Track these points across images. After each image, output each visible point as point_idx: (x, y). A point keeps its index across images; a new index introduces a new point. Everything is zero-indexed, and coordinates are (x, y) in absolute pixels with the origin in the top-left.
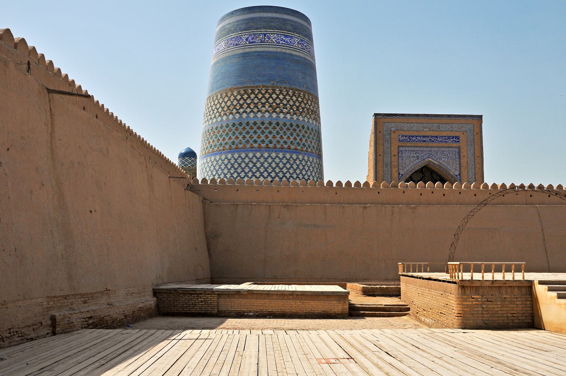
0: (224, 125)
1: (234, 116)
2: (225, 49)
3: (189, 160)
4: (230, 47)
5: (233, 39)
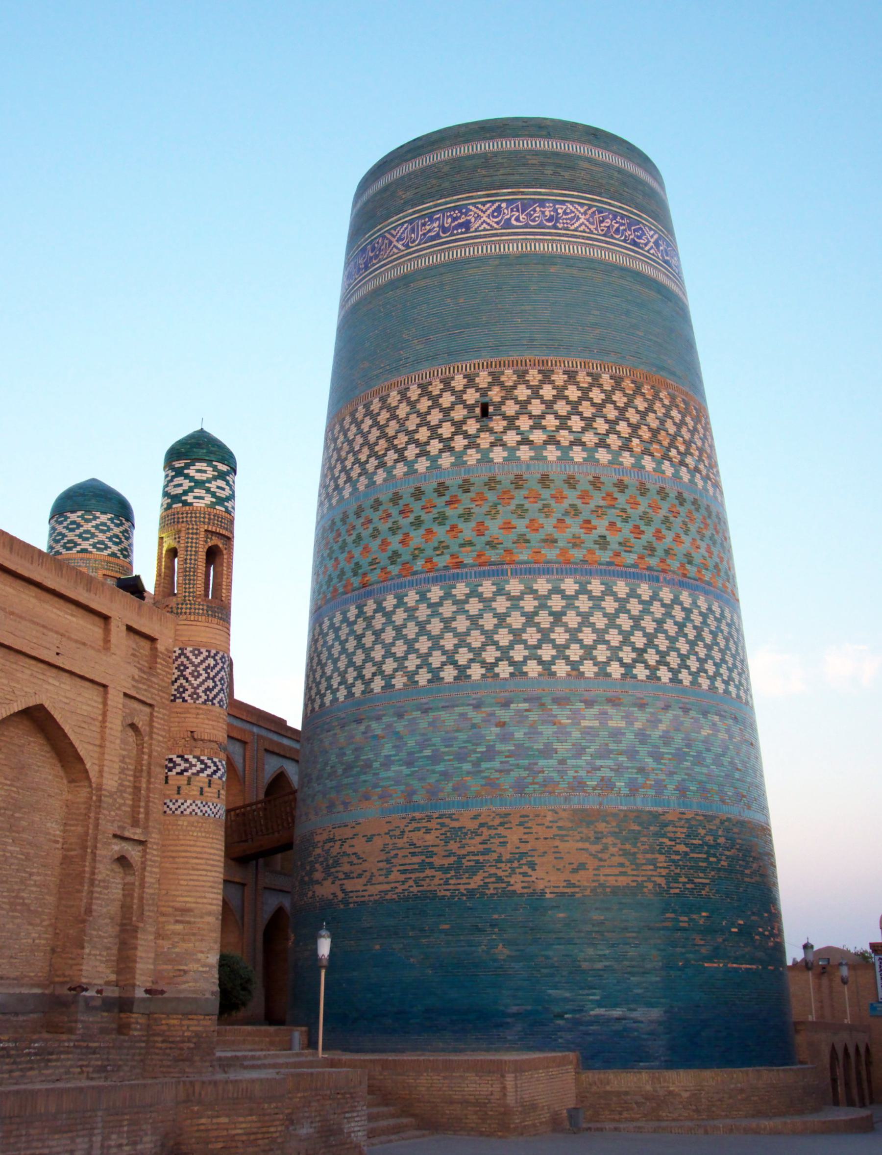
2: (591, 232)
3: (112, 526)
5: (618, 219)
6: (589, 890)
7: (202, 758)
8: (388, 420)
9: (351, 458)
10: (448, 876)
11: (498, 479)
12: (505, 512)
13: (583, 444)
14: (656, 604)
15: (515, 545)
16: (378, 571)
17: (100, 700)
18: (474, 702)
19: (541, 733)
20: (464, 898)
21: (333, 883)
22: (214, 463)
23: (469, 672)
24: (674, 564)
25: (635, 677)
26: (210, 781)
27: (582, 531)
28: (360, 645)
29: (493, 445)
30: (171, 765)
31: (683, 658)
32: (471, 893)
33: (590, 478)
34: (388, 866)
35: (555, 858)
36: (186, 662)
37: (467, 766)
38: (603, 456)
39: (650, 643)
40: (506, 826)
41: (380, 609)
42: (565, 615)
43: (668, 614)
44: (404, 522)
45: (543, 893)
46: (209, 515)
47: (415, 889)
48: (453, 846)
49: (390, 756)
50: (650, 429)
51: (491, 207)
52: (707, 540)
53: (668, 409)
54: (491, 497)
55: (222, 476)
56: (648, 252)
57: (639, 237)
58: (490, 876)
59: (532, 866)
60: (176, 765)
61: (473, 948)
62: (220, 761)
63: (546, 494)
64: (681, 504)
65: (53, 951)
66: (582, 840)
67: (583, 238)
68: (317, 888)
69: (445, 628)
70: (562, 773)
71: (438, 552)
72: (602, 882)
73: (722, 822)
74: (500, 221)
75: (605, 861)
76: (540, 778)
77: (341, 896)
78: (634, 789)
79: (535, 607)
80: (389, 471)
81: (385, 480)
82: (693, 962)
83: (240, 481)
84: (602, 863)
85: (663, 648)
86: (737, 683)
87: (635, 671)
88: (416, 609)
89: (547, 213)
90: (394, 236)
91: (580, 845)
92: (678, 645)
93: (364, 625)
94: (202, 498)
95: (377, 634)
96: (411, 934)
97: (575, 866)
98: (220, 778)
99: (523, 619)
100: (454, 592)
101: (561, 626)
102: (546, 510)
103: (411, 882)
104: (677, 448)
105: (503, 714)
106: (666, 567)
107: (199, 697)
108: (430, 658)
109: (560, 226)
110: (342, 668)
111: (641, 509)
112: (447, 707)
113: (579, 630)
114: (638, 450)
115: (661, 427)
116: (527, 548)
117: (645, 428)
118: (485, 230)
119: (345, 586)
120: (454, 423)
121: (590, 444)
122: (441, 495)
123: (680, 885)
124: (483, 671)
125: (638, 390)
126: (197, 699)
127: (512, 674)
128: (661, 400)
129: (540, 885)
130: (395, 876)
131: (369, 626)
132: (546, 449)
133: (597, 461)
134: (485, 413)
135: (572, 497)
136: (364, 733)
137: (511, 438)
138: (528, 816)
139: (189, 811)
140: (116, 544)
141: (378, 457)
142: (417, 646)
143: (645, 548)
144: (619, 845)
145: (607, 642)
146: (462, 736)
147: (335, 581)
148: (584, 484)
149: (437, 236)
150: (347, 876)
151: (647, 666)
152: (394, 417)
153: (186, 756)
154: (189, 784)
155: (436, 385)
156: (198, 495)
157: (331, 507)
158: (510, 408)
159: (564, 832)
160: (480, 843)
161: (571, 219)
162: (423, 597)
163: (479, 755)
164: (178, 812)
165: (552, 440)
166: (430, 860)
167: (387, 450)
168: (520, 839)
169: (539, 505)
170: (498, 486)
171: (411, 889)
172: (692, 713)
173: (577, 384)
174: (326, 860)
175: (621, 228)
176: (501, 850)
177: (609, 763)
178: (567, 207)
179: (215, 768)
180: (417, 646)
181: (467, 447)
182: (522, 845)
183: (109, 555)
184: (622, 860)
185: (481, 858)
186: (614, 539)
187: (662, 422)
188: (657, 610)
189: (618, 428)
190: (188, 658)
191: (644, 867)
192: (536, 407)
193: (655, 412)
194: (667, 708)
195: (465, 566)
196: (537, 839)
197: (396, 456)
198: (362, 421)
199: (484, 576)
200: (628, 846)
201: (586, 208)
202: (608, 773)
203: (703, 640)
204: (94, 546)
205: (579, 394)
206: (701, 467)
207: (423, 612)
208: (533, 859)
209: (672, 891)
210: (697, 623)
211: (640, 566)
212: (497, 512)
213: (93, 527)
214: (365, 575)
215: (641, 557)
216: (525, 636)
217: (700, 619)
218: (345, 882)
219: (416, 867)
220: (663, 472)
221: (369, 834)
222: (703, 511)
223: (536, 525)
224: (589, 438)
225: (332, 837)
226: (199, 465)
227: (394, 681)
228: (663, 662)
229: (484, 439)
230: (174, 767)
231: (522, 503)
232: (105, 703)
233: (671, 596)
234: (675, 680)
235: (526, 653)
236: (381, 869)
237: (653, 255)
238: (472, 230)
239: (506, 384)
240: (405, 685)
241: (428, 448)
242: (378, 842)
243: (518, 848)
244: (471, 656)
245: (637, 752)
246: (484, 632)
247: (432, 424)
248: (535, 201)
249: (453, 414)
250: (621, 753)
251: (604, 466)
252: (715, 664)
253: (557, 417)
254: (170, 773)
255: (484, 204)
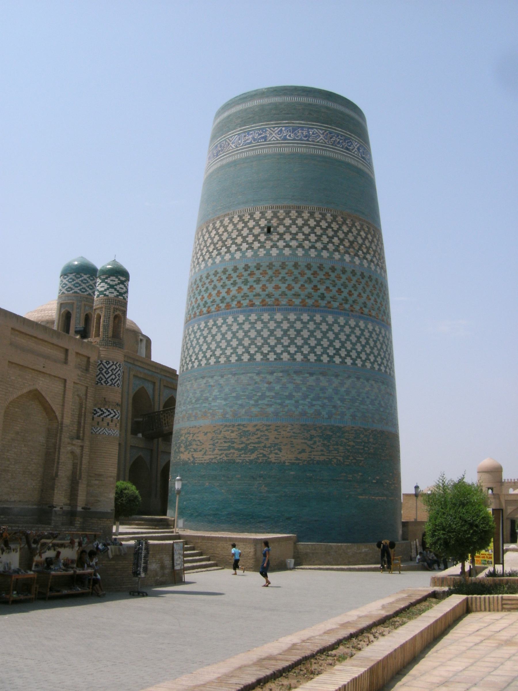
0: (349, 270)
1: (361, 262)
2: (326, 143)
3: (89, 281)
4: (336, 146)
6: (306, 462)
7: (109, 409)
8: (223, 232)
9: (205, 250)
10: (241, 453)
11: (274, 264)
12: (276, 281)
13: (315, 248)
14: (347, 327)
15: (280, 297)
16: (215, 306)
17: (63, 385)
18: (257, 371)
19: (288, 388)
20: (248, 463)
21: (189, 453)
22: (119, 277)
23: (255, 357)
24: (357, 308)
25: (334, 362)
26: (112, 420)
27: (313, 290)
28: (205, 341)
29: (272, 247)
30: (95, 412)
31: (359, 353)
32: (251, 462)
33: (318, 265)
34: (214, 447)
35: (291, 447)
36: (103, 367)
37: (252, 402)
38: (325, 254)
39: (343, 345)
40: (269, 431)
41: (215, 324)
42: (302, 331)
43: (353, 332)
44: (228, 283)
45: (284, 463)
46: (116, 300)
47: (225, 458)
48: (244, 439)
49: (216, 395)
50: (349, 241)
51: (277, 129)
52: (375, 296)
53: (359, 231)
54: (270, 272)
55: (122, 282)
56: (354, 153)
57: (350, 146)
58: (260, 454)
59: (280, 450)
60: (97, 412)
61: (251, 487)
62: (117, 411)
63: (296, 272)
64: (363, 278)
65: (42, 490)
66: (304, 439)
67: (321, 146)
68: (181, 455)
69: (245, 335)
70: (297, 407)
71: (244, 298)
72: (312, 458)
73: (372, 431)
74: (282, 136)
75: (314, 448)
76: (286, 409)
77: (192, 459)
78: (330, 416)
79: (288, 327)
80: (223, 258)
81: (220, 262)
82: (353, 496)
83: (132, 285)
84: (313, 450)
85: (349, 348)
86: (385, 365)
87: (334, 359)
88: (232, 325)
89: (304, 133)
90: (231, 141)
91: (303, 441)
92: (356, 347)
93: (207, 332)
94: (113, 293)
95: (214, 336)
96: (222, 479)
97: (299, 451)
98: (117, 418)
99: (282, 333)
100: (250, 318)
101: (300, 337)
102: (296, 280)
103: (224, 455)
104: (362, 251)
105: (270, 378)
106: (353, 309)
107: (108, 382)
108: (237, 350)
109: (310, 140)
110: (197, 352)
111: (342, 280)
112: (244, 373)
113: (309, 339)
114: (342, 251)
115: (355, 240)
116: (286, 298)
117: (346, 240)
118: (274, 140)
119: (200, 312)
120: (254, 236)
121: (319, 248)
122: (246, 270)
123: (350, 461)
124: (262, 357)
125: (344, 222)
126: (107, 383)
127: (275, 359)
128: (356, 227)
129: (283, 459)
130: (216, 452)
131: (210, 332)
132: (297, 250)
133: (322, 256)
134: (269, 231)
135: (309, 273)
136: (205, 384)
137: (281, 244)
138: (279, 427)
139: (102, 432)
140: (91, 289)
141: (218, 250)
142: (231, 343)
143: (343, 300)
144: (322, 442)
145: (322, 345)
146: (250, 388)
147: (195, 309)
148: (315, 268)
149: (251, 143)
150: (195, 450)
151: (341, 357)
152: (226, 230)
153: (102, 409)
154: (103, 420)
155: (247, 216)
156: (111, 291)
157: (195, 273)
158: (281, 229)
159: (296, 435)
160: (257, 439)
161: (316, 137)
162: (235, 320)
163: (258, 397)
164: (98, 433)
165: (300, 246)
166: (233, 445)
167: (222, 247)
168: (275, 437)
169: (293, 278)
170: (274, 268)
171: (224, 458)
172: (361, 380)
173: (314, 218)
174: (186, 442)
175: (341, 141)
176: (266, 442)
177: (319, 403)
178: (314, 131)
179: (115, 414)
180: (231, 343)
181: (259, 248)
182: (275, 440)
183: (87, 294)
184: (322, 448)
185: (256, 445)
186: (328, 295)
187: (356, 238)
188: (347, 330)
189: (333, 241)
190: (104, 365)
191: (333, 452)
192: (294, 229)
193: (352, 233)
194: (349, 377)
195: (256, 306)
196: (283, 437)
197: (226, 250)
198: (211, 232)
199: (265, 311)
200: (326, 442)
201: (324, 131)
202: (318, 408)
203: (369, 344)
204: (80, 290)
205: (315, 223)
206: (374, 259)
207: (235, 328)
208: (281, 446)
209: (346, 463)
210: (367, 336)
211: (340, 308)
212: (272, 280)
213: (80, 281)
214: (209, 307)
215: (341, 304)
216: (282, 341)
217: (369, 334)
218: (194, 453)
219: (226, 448)
220: (355, 263)
221: (206, 432)
222: (374, 282)
223: (291, 287)
224: (319, 245)
225: (189, 432)
226: (112, 278)
227: (220, 360)
228: (348, 355)
229: (268, 244)
230: (96, 413)
231: (284, 276)
232: (65, 387)
233: (355, 323)
234: (354, 364)
235: (283, 349)
236: (211, 448)
237: (356, 154)
238: (267, 140)
239: (280, 217)
240: (225, 362)
241: (241, 247)
242: (210, 436)
243: (274, 441)
244: (256, 349)
245: (333, 398)
246: (263, 338)
247: (244, 235)
248: (299, 127)
249: (254, 231)
250: (326, 398)
251: (325, 259)
252: (374, 356)
253: (304, 234)
254: (95, 416)
255: (274, 128)
